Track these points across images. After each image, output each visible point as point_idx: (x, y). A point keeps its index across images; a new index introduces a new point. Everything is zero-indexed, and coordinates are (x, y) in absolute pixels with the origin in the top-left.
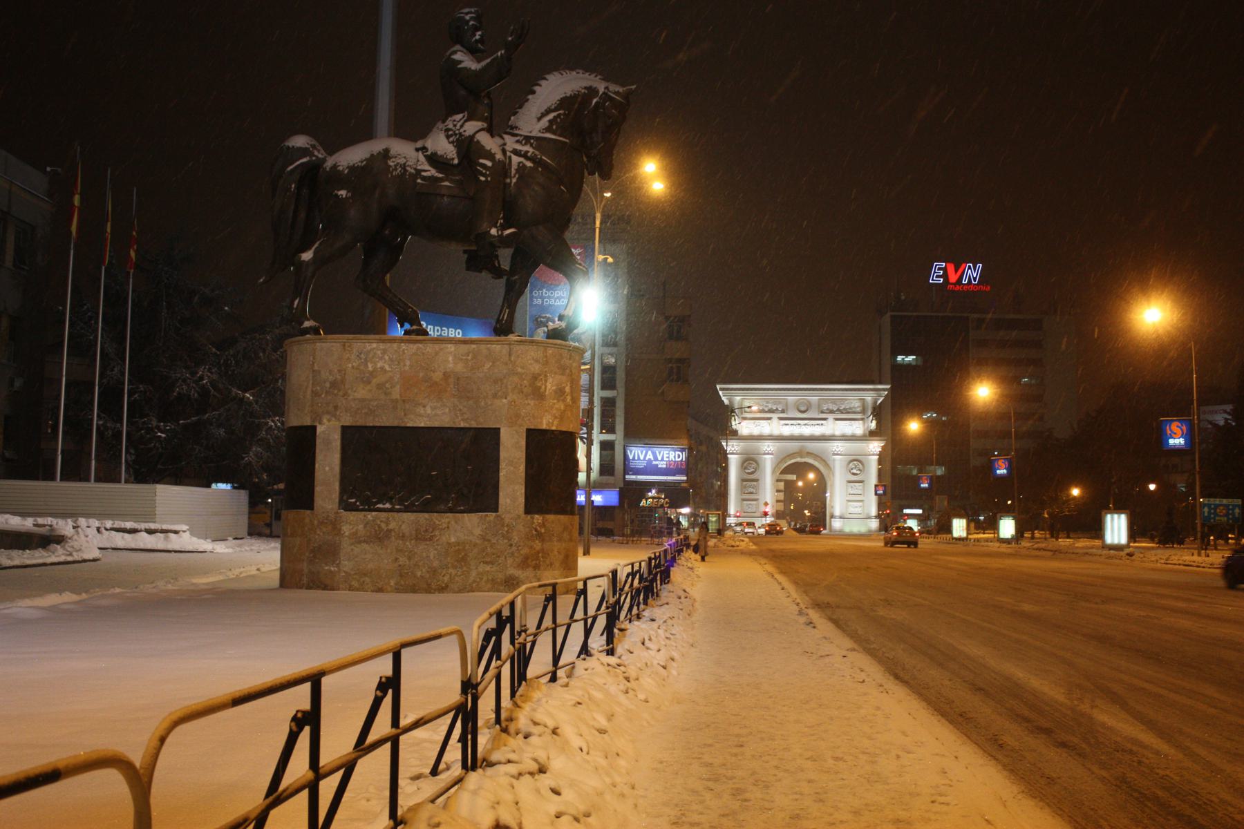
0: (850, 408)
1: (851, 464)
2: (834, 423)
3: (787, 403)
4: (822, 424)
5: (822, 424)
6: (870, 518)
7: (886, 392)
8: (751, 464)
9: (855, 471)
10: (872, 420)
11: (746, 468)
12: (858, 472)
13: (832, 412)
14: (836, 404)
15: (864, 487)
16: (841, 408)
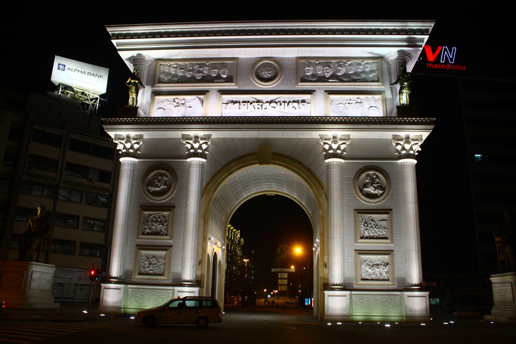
0: (356, 74)
1: (364, 175)
2: (326, 99)
3: (237, 66)
4: (303, 101)
5: (303, 101)
6: (408, 288)
7: (426, 38)
8: (162, 175)
9: (371, 190)
10: (402, 88)
11: (151, 183)
12: (379, 192)
13: (322, 79)
14: (329, 66)
15: (391, 221)
16: (338, 74)
